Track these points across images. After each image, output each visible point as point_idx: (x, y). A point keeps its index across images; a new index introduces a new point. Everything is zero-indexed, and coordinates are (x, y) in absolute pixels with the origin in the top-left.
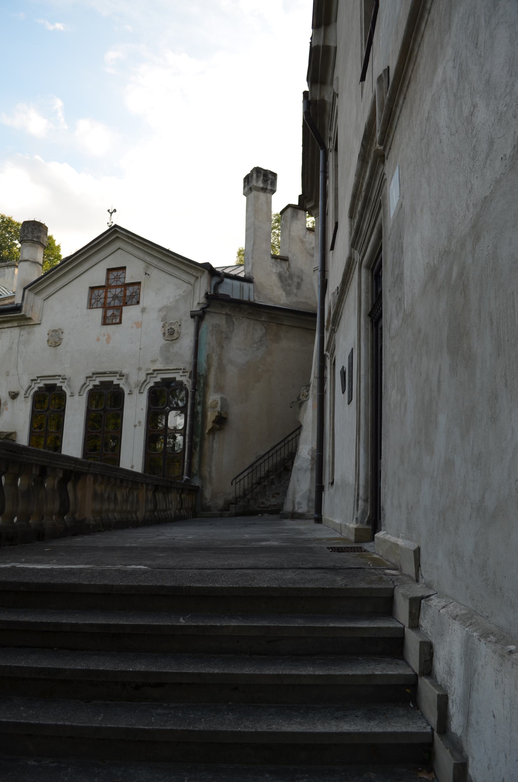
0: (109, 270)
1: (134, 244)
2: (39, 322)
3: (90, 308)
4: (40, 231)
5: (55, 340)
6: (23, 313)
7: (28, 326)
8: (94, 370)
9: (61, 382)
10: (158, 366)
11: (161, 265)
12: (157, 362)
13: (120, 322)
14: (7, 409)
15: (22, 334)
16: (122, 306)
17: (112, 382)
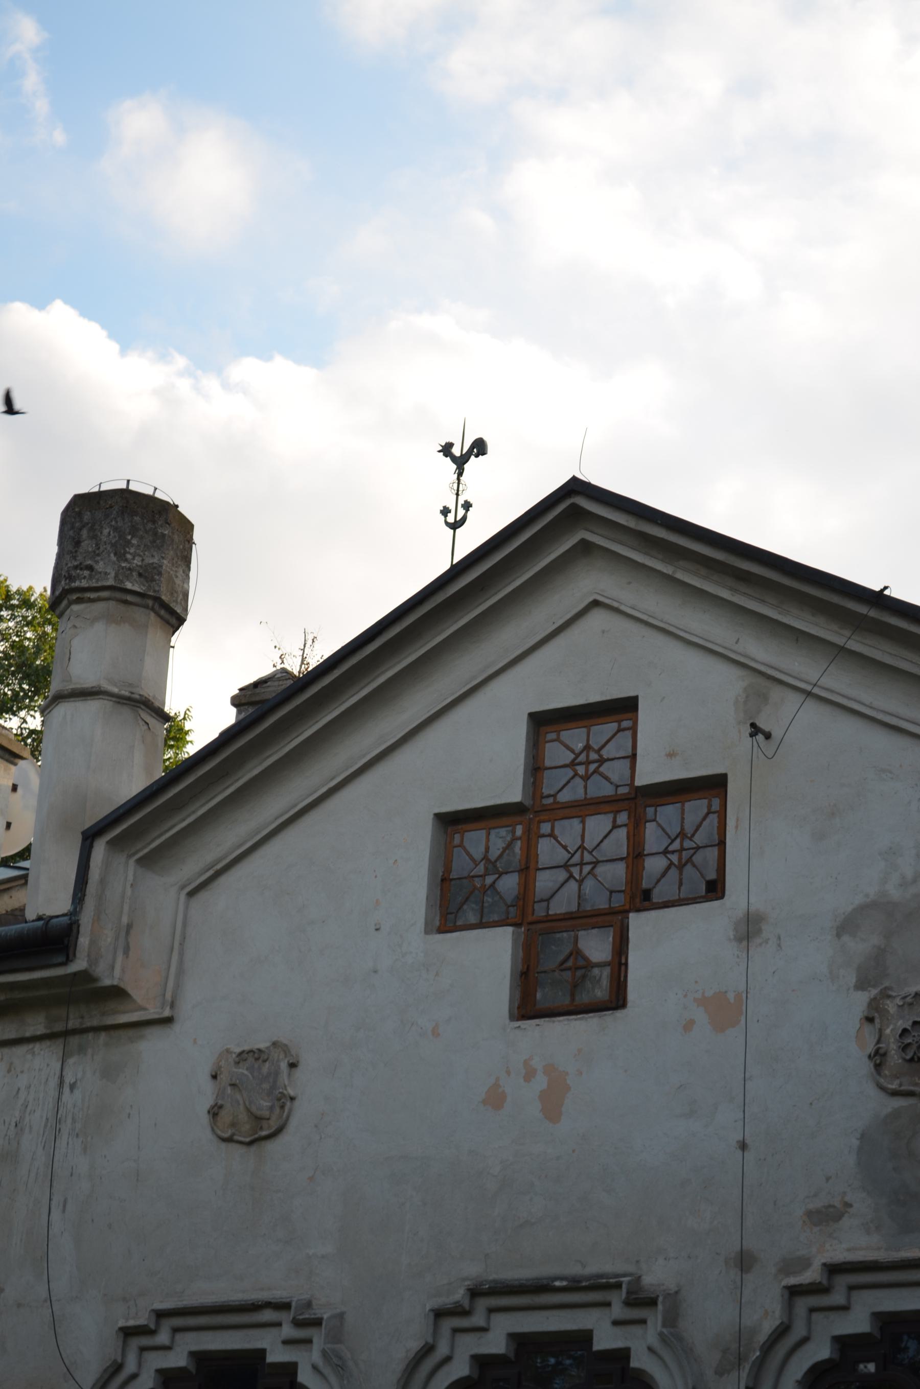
0: (543, 723)
1: (679, 575)
2: (167, 1013)
3: (442, 930)
4: (158, 542)
5: (254, 1103)
6: (79, 965)
7: (103, 1036)
8: (473, 1270)
9: (286, 1342)
10: (854, 1242)
11: (840, 681)
12: (846, 1222)
13: (617, 1000)
15: (69, 1079)
16: (625, 912)
17: (586, 1337)
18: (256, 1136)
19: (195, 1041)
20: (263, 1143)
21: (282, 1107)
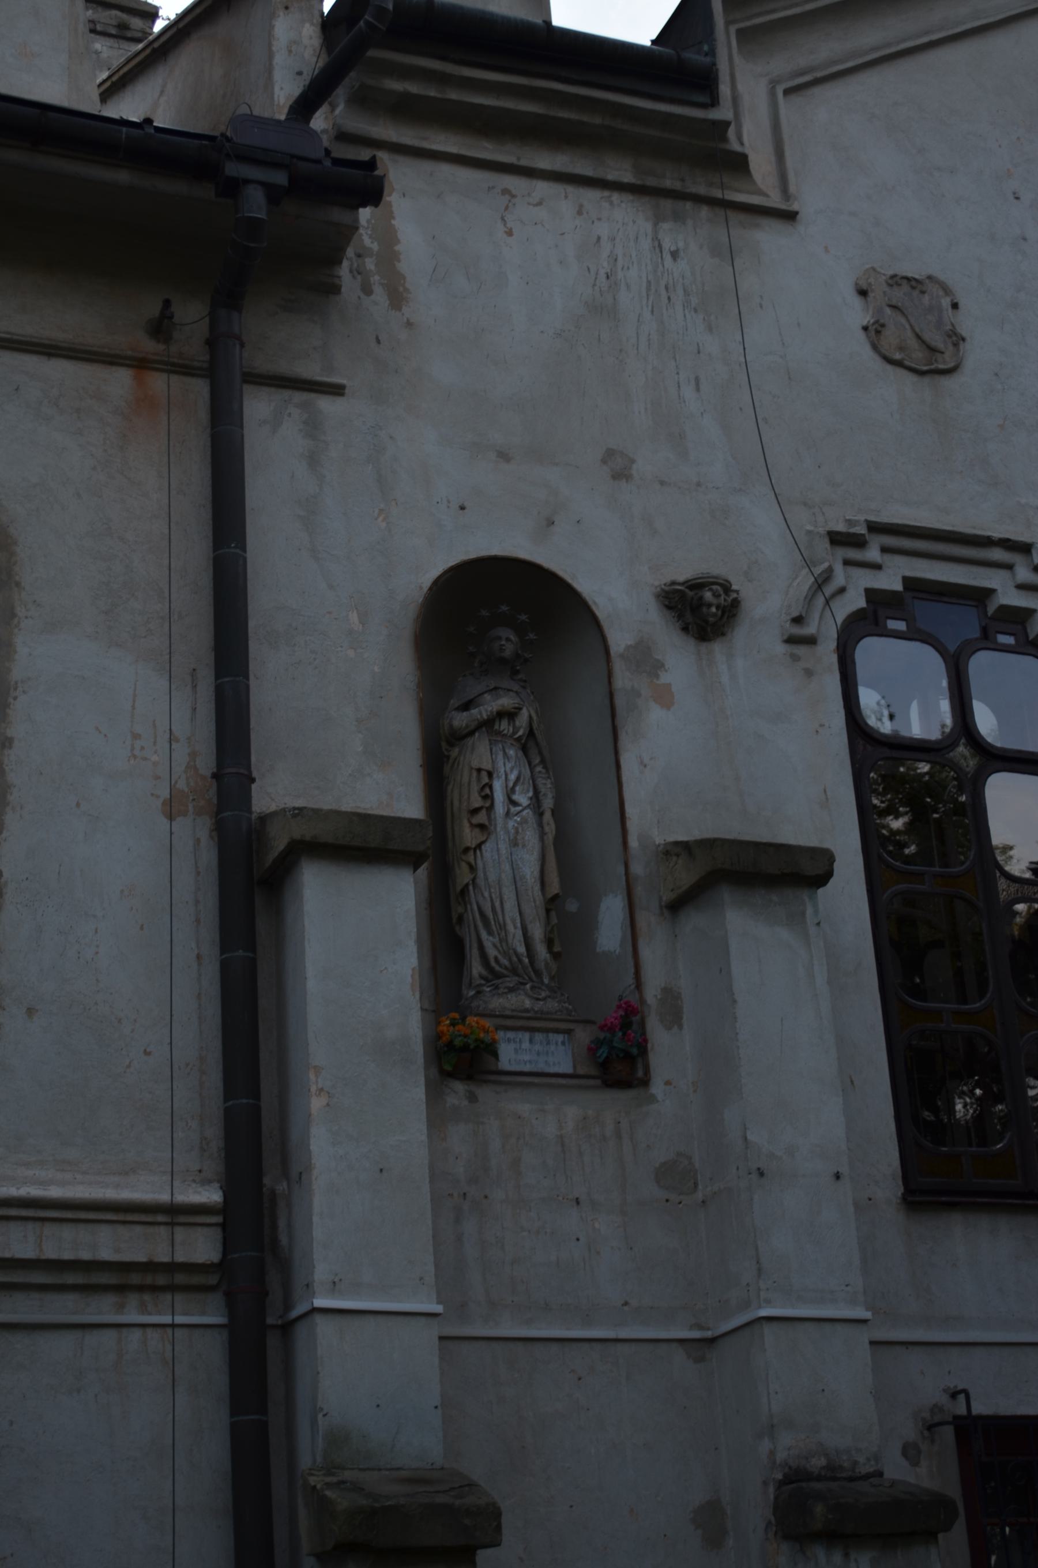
7: (705, 211)
9: (1022, 587)
14: (665, 698)
15: (667, 245)
18: (932, 367)
20: (937, 377)
21: (956, 345)
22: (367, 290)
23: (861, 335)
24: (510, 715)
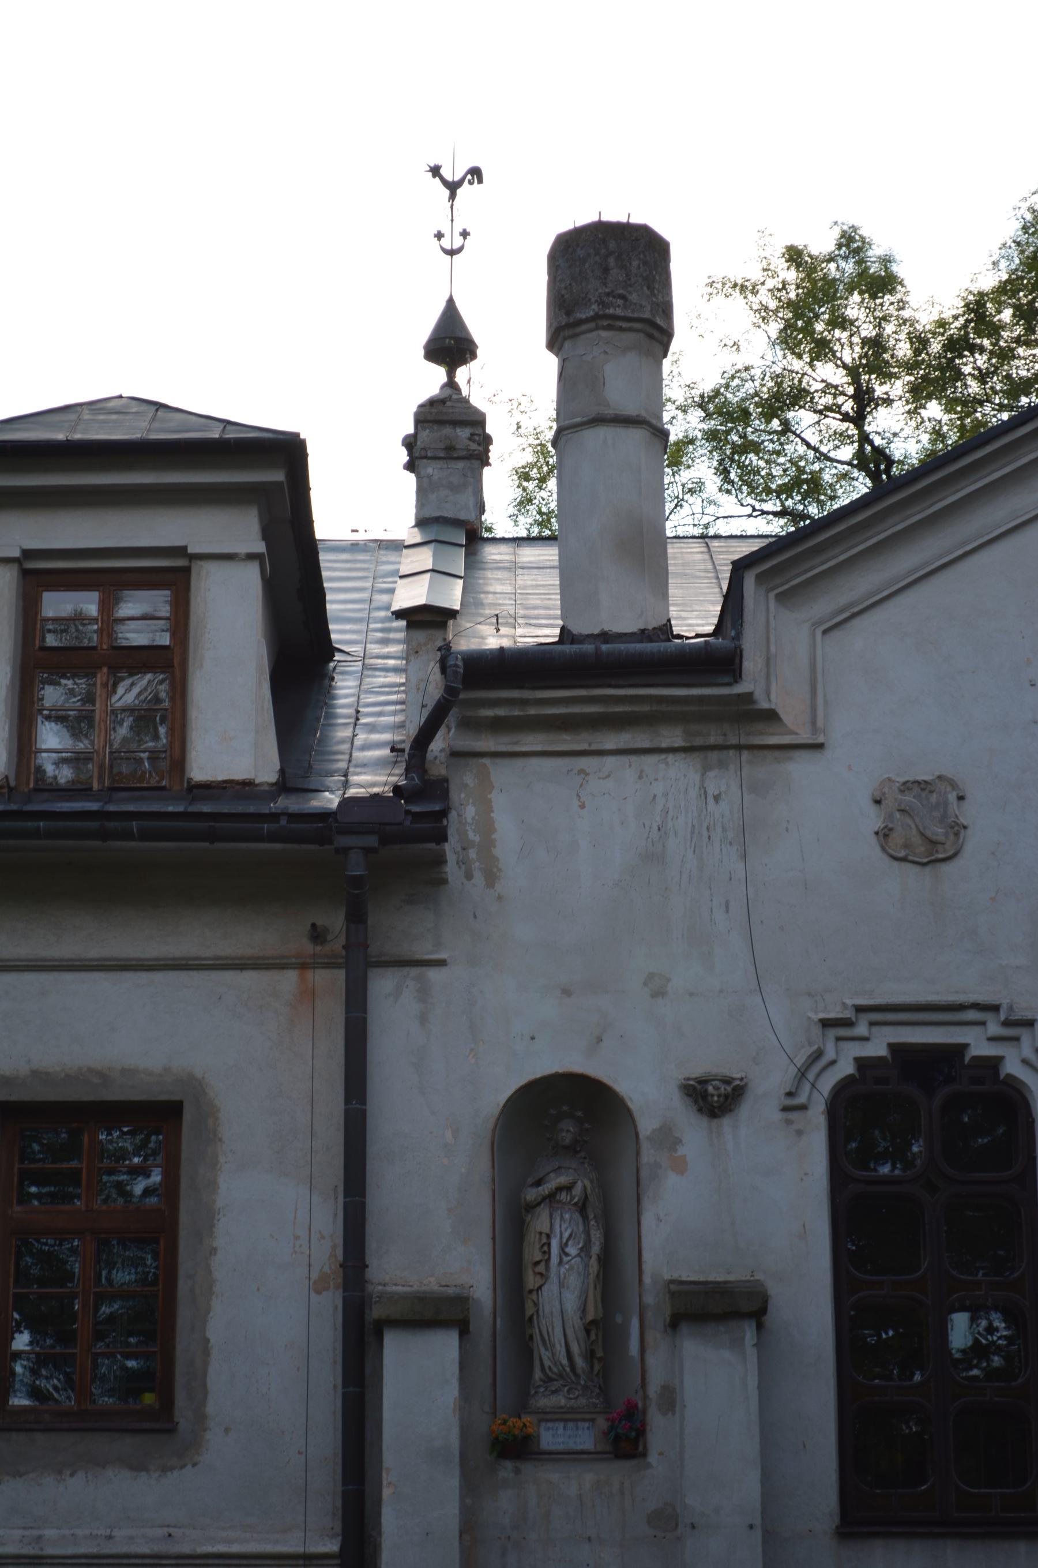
7: (745, 755)
9: (991, 1039)
14: (680, 1166)
15: (712, 790)
18: (933, 858)
19: (850, 767)
20: (938, 865)
21: (957, 834)
22: (469, 876)
23: (873, 840)
24: (569, 1188)
